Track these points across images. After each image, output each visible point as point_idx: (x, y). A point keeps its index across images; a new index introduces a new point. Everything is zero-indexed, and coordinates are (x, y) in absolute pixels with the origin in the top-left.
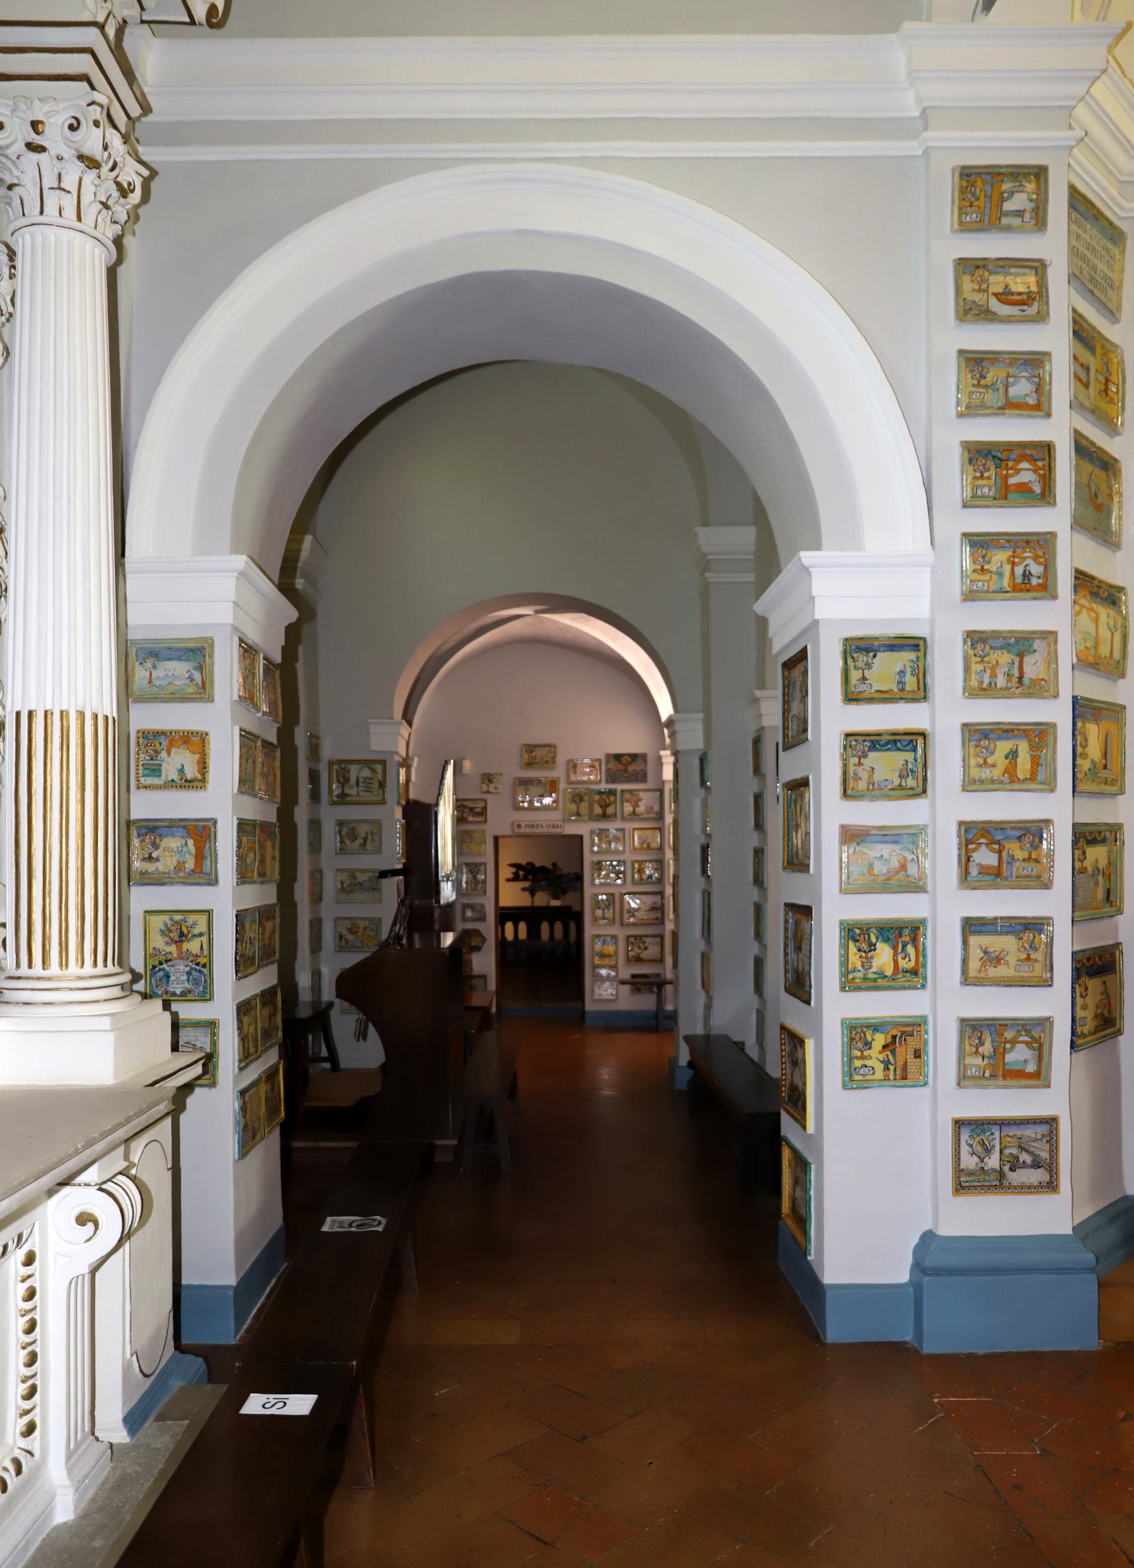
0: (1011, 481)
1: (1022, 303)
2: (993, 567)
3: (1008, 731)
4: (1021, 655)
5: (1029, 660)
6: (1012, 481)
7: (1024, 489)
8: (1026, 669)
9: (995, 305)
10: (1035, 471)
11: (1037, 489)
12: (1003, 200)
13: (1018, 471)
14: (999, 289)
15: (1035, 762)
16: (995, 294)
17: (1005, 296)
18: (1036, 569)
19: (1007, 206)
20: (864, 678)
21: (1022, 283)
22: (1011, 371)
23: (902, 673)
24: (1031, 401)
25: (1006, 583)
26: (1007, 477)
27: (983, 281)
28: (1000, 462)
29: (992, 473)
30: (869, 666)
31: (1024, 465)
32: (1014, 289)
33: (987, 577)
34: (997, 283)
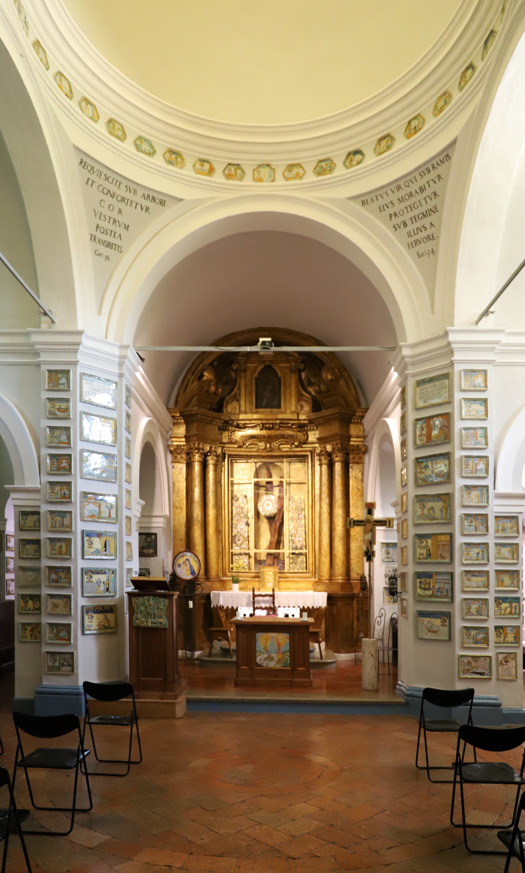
0: (61, 466)
1: (64, 412)
2: (55, 491)
3: (60, 540)
4: (63, 518)
5: (65, 519)
6: (61, 466)
7: (64, 468)
8: (65, 522)
9: (57, 412)
10: (67, 463)
11: (68, 468)
12: (59, 380)
13: (62, 463)
14: (58, 407)
15: (67, 550)
16: (57, 409)
17: (59, 409)
18: (67, 492)
19: (60, 382)
20: (25, 523)
21: (63, 406)
22: (61, 432)
23: (35, 521)
24: (66, 441)
25: (59, 496)
26: (59, 464)
27: (54, 405)
28: (58, 460)
29: (55, 463)
30: (26, 519)
31: (64, 461)
32: (62, 407)
33: (53, 494)
34: (57, 405)
